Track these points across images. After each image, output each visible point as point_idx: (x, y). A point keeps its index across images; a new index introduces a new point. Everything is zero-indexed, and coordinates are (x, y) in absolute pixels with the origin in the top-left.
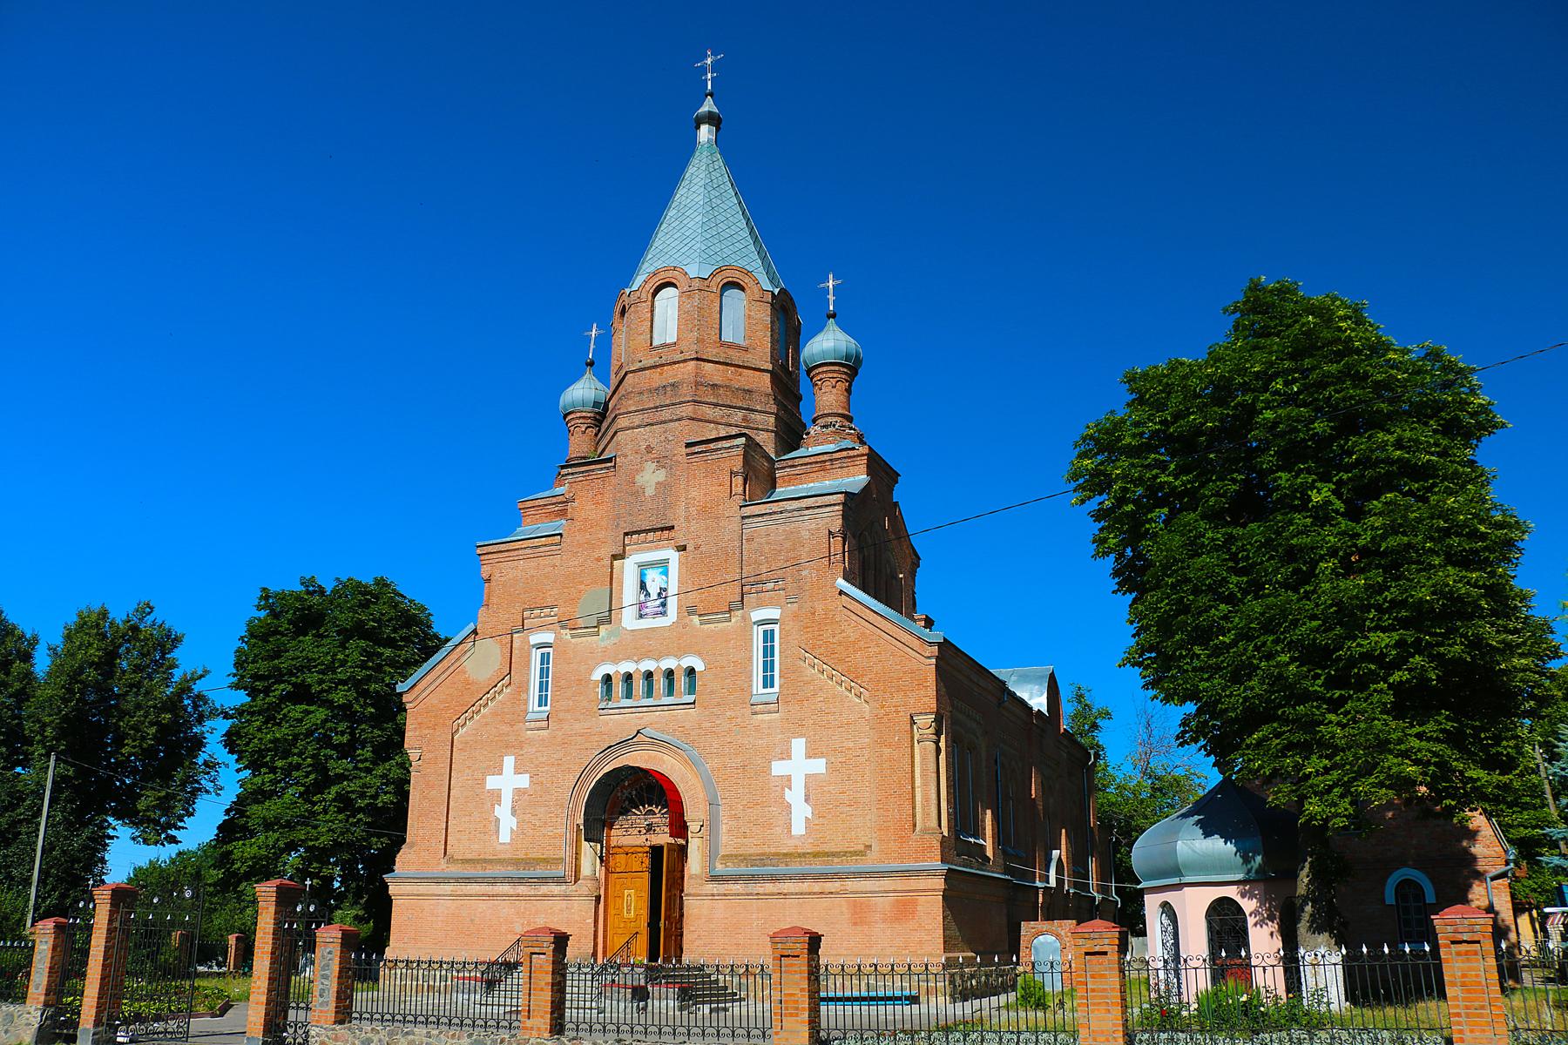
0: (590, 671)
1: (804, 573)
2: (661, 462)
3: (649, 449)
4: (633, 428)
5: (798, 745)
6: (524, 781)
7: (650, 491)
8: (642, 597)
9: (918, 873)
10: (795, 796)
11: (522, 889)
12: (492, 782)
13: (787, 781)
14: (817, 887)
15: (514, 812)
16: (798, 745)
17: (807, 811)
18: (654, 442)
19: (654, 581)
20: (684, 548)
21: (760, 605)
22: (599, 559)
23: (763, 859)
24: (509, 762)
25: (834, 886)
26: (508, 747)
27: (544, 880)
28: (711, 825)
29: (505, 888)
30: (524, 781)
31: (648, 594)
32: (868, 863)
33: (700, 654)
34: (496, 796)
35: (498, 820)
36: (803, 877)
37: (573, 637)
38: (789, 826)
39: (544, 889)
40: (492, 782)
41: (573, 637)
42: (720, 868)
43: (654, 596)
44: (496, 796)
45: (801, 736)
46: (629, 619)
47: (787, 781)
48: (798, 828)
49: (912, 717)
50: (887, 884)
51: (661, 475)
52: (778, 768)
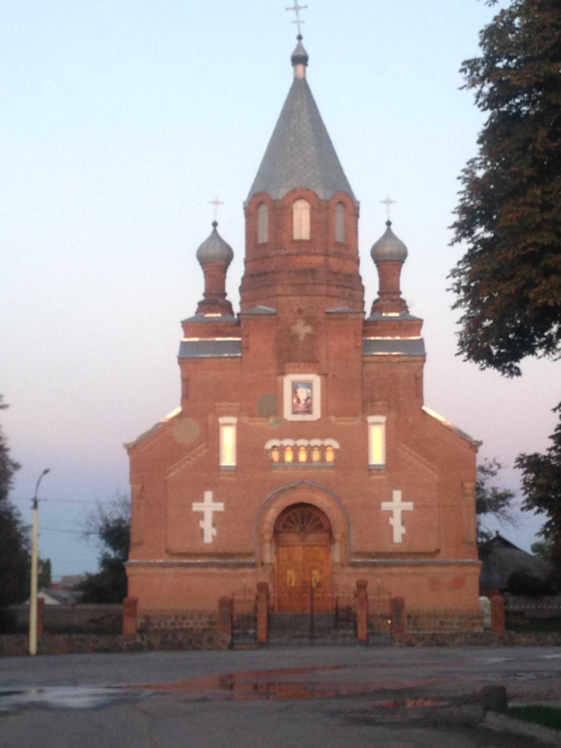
0: (264, 443)
1: (401, 399)
2: (309, 320)
3: (300, 311)
4: (287, 295)
5: (397, 494)
6: (220, 507)
7: (302, 338)
8: (295, 401)
9: (467, 564)
10: (396, 522)
11: (225, 571)
12: (196, 507)
13: (390, 513)
14: (411, 570)
15: (214, 525)
16: (397, 494)
17: (403, 530)
18: (303, 307)
19: (303, 394)
20: (326, 375)
21: (373, 413)
22: (268, 376)
23: (378, 555)
24: (208, 495)
25: (419, 570)
26: (207, 486)
27: (242, 565)
28: (346, 536)
29: (214, 570)
30: (220, 507)
31: (299, 401)
32: (441, 558)
33: (335, 438)
34: (200, 515)
35: (202, 530)
36: (403, 565)
37: (250, 421)
38: (392, 537)
39: (241, 571)
40: (196, 507)
41: (250, 421)
42: (353, 560)
43: (303, 402)
44: (200, 515)
45: (399, 489)
46: (288, 415)
47: (390, 513)
48: (397, 538)
49: (462, 484)
50: (449, 569)
51: (308, 329)
52: (385, 506)
